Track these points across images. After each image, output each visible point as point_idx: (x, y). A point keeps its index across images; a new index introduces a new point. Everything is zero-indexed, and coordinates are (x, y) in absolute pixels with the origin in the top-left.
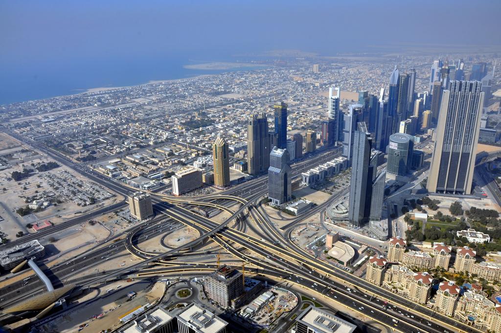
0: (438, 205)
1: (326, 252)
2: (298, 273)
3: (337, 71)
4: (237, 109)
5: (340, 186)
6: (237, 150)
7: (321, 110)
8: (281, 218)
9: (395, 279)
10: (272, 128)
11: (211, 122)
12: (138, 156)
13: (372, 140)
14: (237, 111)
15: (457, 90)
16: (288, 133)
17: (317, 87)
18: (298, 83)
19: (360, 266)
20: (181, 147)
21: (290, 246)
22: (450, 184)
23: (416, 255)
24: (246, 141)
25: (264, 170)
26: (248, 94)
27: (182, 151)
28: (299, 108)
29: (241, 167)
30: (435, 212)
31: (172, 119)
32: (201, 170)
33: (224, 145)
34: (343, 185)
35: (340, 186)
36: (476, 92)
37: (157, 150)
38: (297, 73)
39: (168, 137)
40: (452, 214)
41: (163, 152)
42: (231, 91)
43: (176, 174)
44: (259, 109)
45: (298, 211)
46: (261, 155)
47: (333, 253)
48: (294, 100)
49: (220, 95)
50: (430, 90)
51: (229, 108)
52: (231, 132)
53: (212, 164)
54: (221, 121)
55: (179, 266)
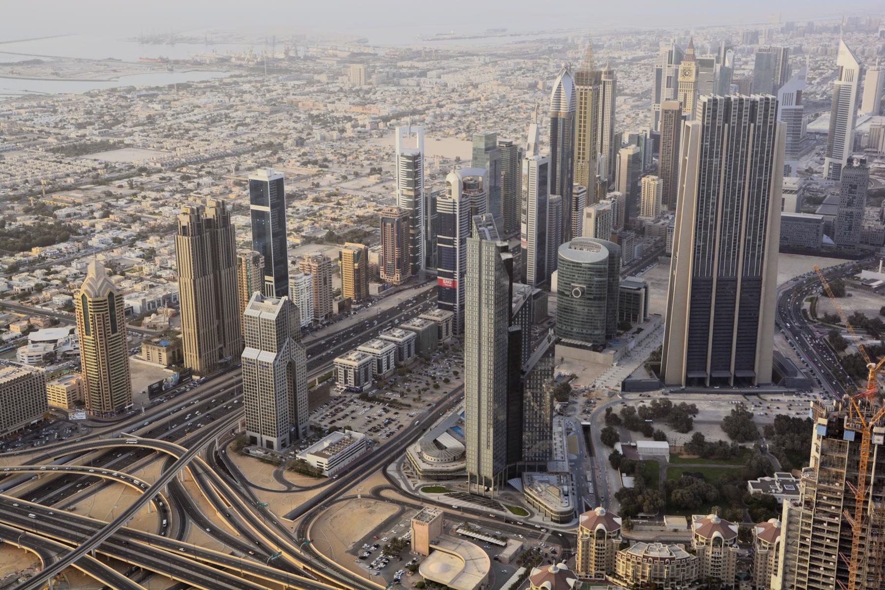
1: (415, 569)
3: (412, 82)
4: (143, 194)
6: (150, 309)
7: (378, 189)
8: (285, 488)
13: (511, 260)
14: (144, 197)
15: (719, 121)
16: (290, 253)
17: (364, 126)
18: (311, 116)
21: (315, 561)
22: (721, 362)
23: (653, 554)
24: (174, 280)
25: (229, 358)
26: (175, 149)
28: (318, 185)
29: (164, 356)
30: (688, 437)
32: (42, 370)
33: (111, 295)
34: (447, 381)
36: (765, 122)
38: (307, 89)
40: (732, 436)
42: (122, 142)
44: (205, 191)
45: (331, 464)
46: (218, 317)
48: (305, 164)
50: (653, 126)
51: (119, 191)
52: (131, 256)
53: (76, 352)
54: (99, 227)
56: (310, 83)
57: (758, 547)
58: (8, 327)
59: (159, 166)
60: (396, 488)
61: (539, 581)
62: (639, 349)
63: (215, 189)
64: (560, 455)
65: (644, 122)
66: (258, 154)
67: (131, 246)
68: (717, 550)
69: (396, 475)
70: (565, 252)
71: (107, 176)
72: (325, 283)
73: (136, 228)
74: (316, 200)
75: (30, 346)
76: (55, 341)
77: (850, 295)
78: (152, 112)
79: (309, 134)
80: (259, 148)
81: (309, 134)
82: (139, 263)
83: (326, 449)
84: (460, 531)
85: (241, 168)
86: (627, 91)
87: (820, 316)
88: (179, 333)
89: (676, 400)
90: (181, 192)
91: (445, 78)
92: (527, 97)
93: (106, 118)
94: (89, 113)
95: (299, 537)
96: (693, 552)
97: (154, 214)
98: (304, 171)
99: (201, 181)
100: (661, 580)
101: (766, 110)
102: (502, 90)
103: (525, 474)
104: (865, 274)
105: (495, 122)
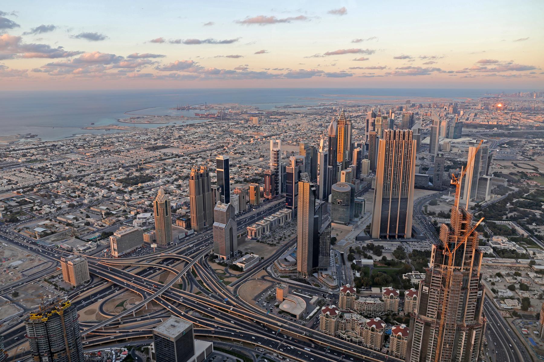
0: (383, 251)
1: (278, 306)
2: (250, 331)
3: (275, 123)
5: (285, 238)
7: (263, 163)
8: (229, 275)
9: (348, 328)
10: (214, 183)
11: (151, 178)
12: (71, 217)
14: (177, 166)
16: (230, 186)
19: (311, 317)
20: (118, 205)
24: (187, 196)
25: (208, 226)
26: (188, 148)
27: (120, 209)
29: (184, 224)
30: (379, 258)
31: (108, 176)
33: (166, 201)
35: (285, 238)
36: (408, 140)
37: (92, 208)
38: (236, 126)
39: (104, 194)
41: (99, 210)
43: (115, 234)
44: (199, 163)
45: (246, 267)
46: (204, 211)
47: (284, 306)
48: (235, 154)
49: (158, 149)
52: (172, 187)
53: (153, 222)
54: (161, 176)
55: (122, 334)
56: (238, 124)
57: (406, 298)
58: (130, 212)
59: (182, 154)
60: (270, 275)
61: (325, 311)
62: (362, 224)
63: (202, 163)
64: (332, 265)
65: (362, 139)
66: (219, 150)
67: (172, 183)
68: (391, 300)
69: (270, 271)
70: (334, 187)
71: (164, 158)
72: (243, 198)
73: (174, 177)
74: (240, 167)
75: (138, 219)
76: (146, 218)
77: (439, 205)
78: (181, 135)
79: (237, 142)
80: (218, 148)
81: (237, 142)
82: (175, 190)
83: (244, 261)
84: (295, 292)
85: (212, 155)
86: (356, 128)
87: (428, 212)
88: (190, 216)
89: (376, 244)
90: (191, 164)
91: (288, 122)
92: (318, 129)
93: (164, 137)
94: (159, 135)
95: (234, 293)
96: (383, 301)
97: (181, 172)
98: (235, 156)
99: (197, 160)
100: (370, 311)
101: (409, 135)
102: (309, 127)
103: (319, 271)
104: (444, 197)
105: (307, 139)
